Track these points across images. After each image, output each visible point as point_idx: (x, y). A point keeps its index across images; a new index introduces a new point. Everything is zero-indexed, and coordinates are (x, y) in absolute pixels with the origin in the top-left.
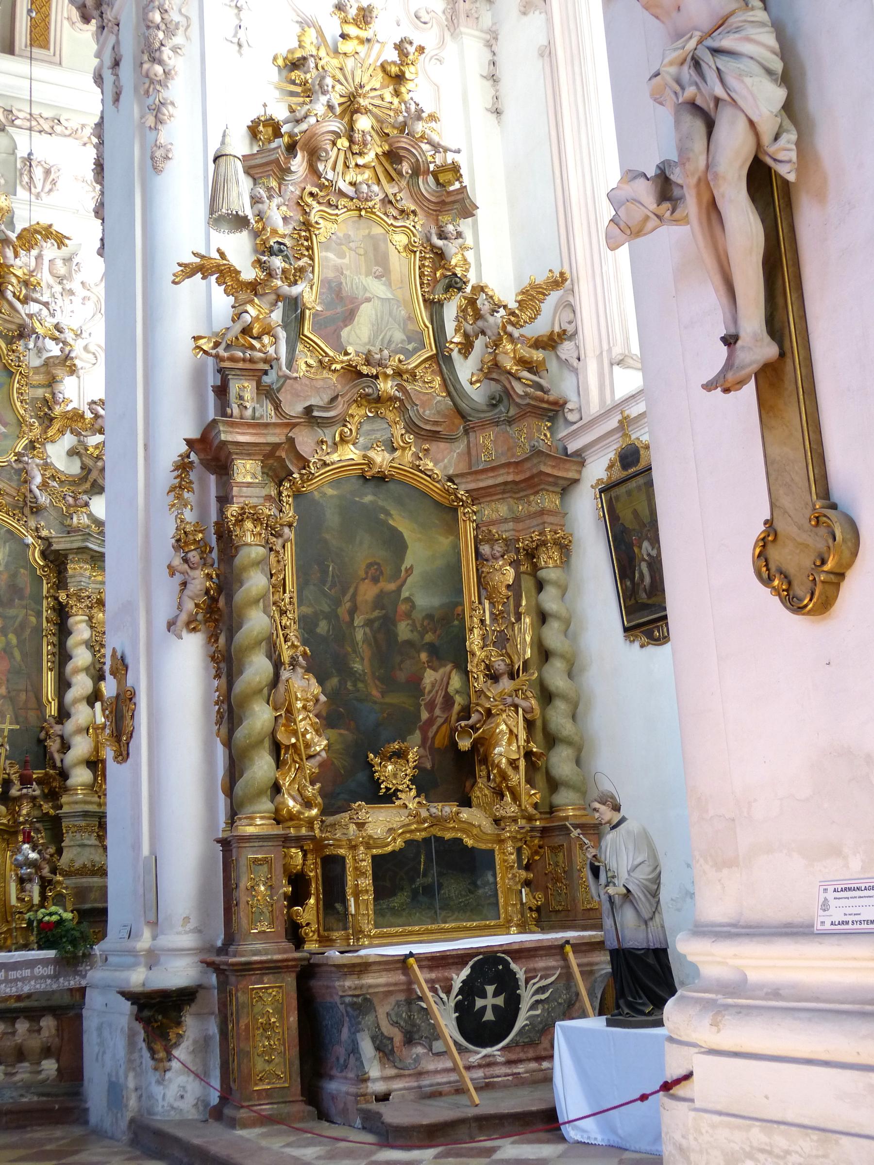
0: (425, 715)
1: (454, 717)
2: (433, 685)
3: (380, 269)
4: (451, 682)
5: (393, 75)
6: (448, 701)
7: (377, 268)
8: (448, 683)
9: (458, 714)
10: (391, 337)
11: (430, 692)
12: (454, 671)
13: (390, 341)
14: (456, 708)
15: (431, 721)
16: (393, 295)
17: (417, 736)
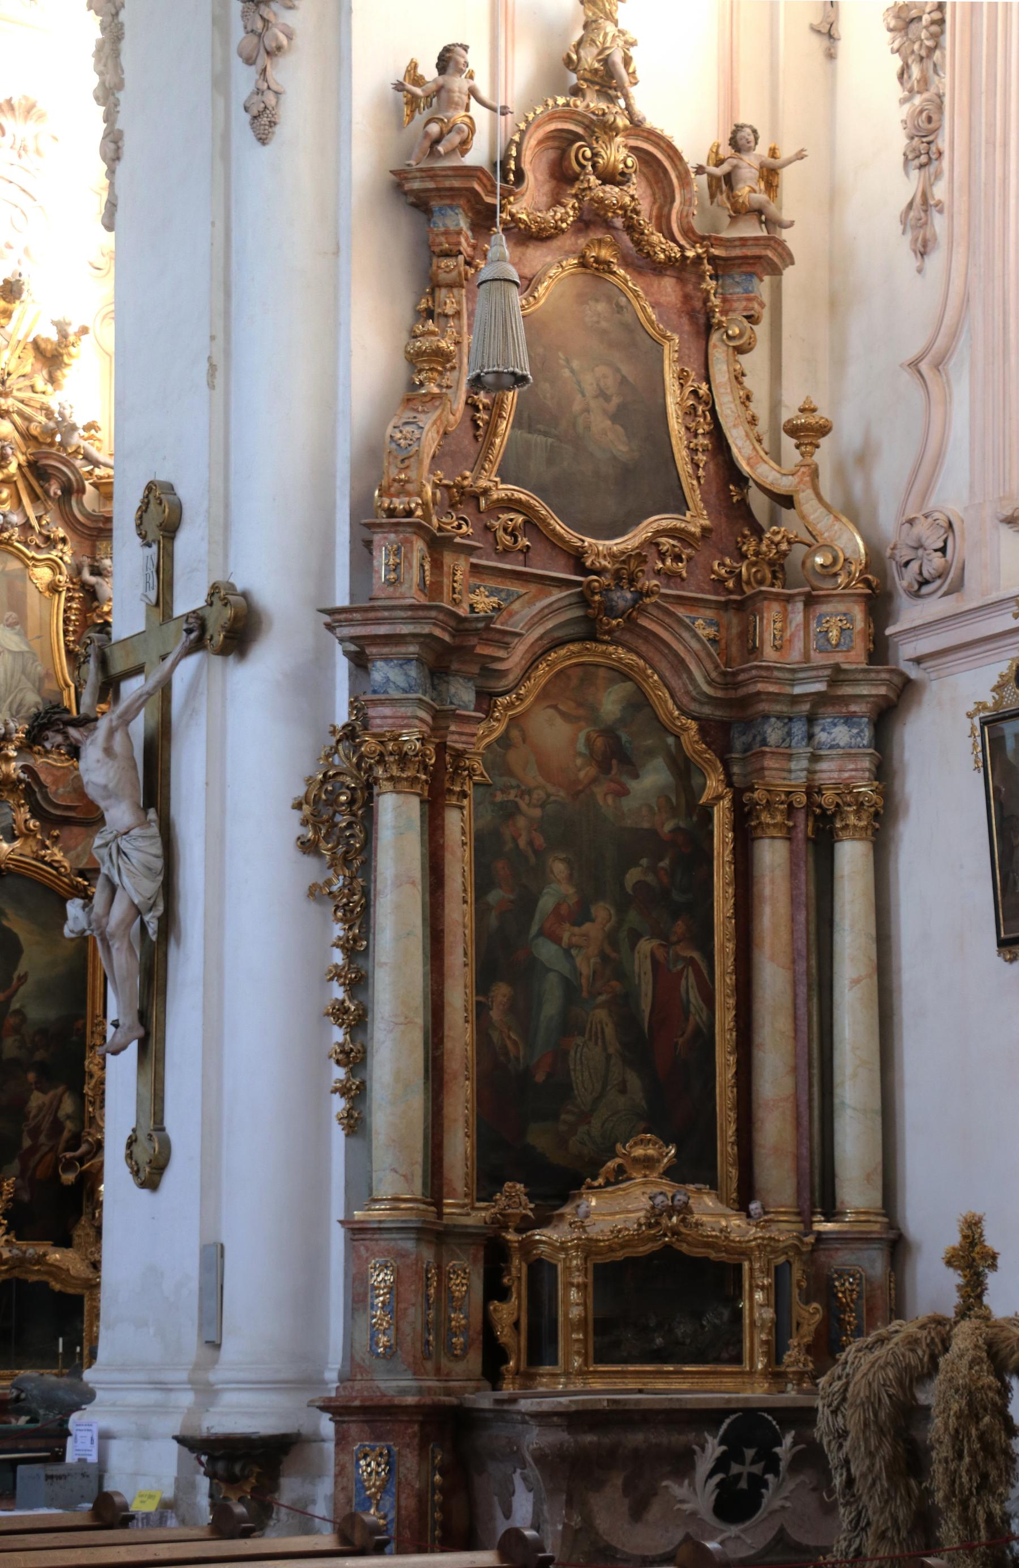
0: (27, 1143)
1: (61, 1146)
2: (40, 1109)
3: (14, 615)
4: (63, 1106)
5: (48, 355)
6: (57, 1127)
7: (9, 614)
8: (58, 1108)
9: (67, 1142)
10: (22, 700)
11: (36, 1116)
12: (66, 1095)
13: (20, 705)
14: (66, 1134)
15: (33, 1150)
16: (29, 646)
17: (16, 1165)
